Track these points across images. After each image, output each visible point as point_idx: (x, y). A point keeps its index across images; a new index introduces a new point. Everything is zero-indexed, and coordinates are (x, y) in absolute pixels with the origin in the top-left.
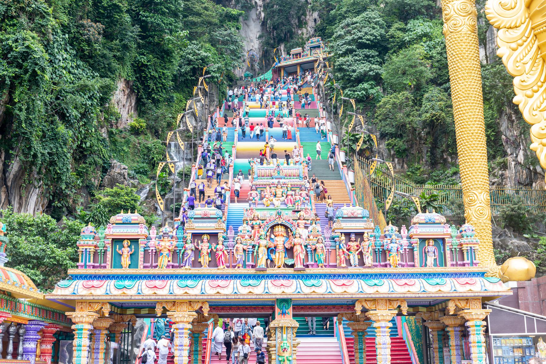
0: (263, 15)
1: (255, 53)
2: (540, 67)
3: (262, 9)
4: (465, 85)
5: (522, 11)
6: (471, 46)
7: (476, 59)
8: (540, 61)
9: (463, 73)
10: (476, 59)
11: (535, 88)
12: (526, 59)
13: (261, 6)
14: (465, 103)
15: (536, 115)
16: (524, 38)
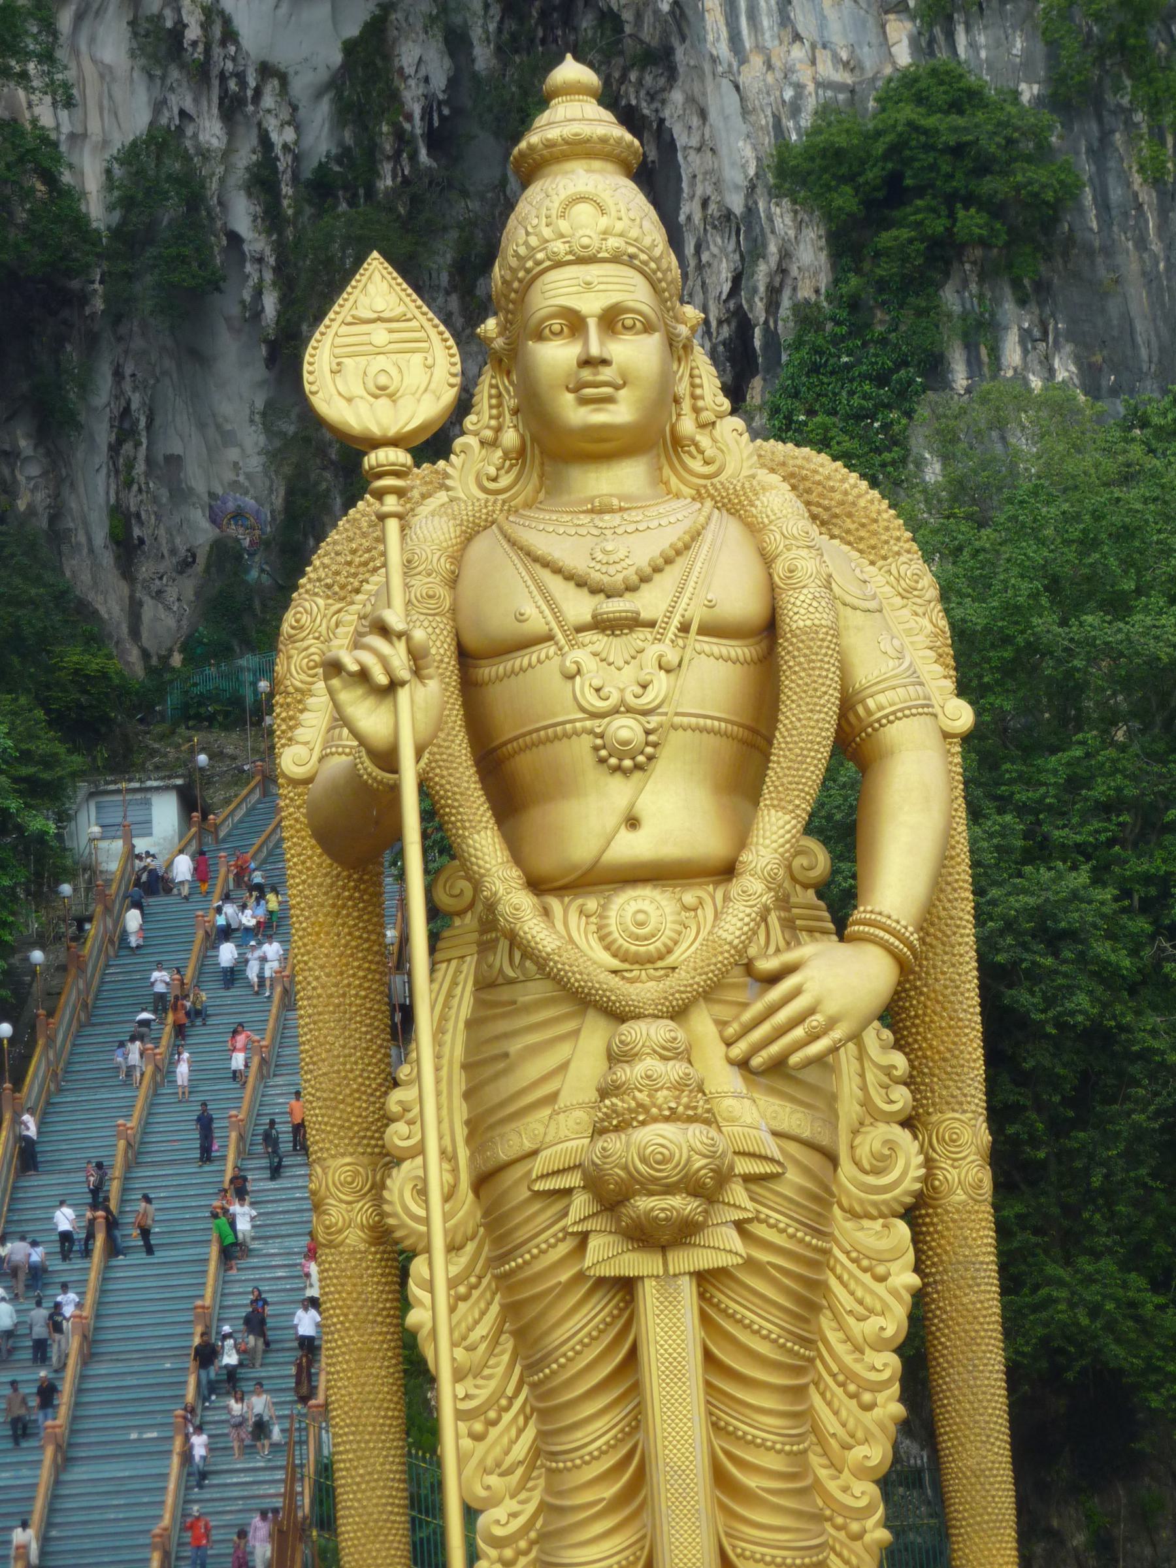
0: (270, 303)
1: (249, 502)
2: (506, 1358)
3: (268, 276)
4: (350, 1394)
5: (466, 1207)
6: (366, 1284)
7: (379, 1319)
8: (508, 1343)
9: (347, 1362)
10: (379, 1319)
11: (492, 1414)
12: (475, 1336)
13: (260, 260)
14: (351, 1442)
15: (488, 1488)
16: (473, 1280)
